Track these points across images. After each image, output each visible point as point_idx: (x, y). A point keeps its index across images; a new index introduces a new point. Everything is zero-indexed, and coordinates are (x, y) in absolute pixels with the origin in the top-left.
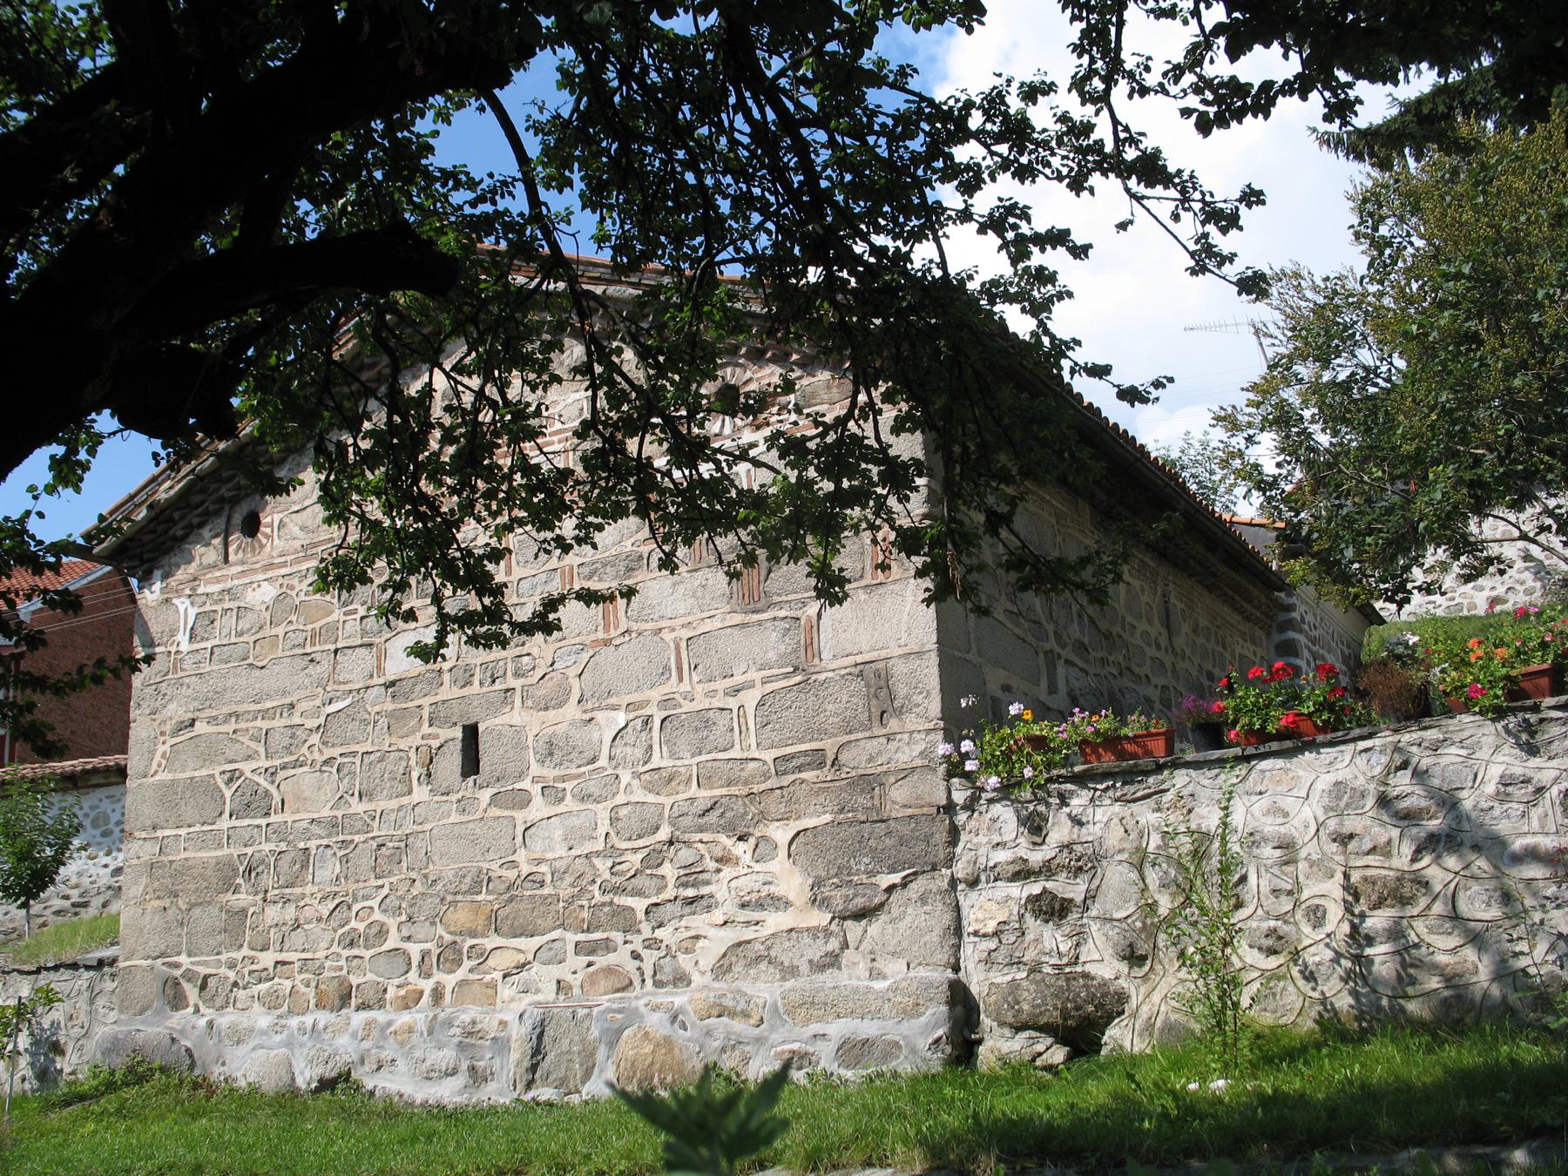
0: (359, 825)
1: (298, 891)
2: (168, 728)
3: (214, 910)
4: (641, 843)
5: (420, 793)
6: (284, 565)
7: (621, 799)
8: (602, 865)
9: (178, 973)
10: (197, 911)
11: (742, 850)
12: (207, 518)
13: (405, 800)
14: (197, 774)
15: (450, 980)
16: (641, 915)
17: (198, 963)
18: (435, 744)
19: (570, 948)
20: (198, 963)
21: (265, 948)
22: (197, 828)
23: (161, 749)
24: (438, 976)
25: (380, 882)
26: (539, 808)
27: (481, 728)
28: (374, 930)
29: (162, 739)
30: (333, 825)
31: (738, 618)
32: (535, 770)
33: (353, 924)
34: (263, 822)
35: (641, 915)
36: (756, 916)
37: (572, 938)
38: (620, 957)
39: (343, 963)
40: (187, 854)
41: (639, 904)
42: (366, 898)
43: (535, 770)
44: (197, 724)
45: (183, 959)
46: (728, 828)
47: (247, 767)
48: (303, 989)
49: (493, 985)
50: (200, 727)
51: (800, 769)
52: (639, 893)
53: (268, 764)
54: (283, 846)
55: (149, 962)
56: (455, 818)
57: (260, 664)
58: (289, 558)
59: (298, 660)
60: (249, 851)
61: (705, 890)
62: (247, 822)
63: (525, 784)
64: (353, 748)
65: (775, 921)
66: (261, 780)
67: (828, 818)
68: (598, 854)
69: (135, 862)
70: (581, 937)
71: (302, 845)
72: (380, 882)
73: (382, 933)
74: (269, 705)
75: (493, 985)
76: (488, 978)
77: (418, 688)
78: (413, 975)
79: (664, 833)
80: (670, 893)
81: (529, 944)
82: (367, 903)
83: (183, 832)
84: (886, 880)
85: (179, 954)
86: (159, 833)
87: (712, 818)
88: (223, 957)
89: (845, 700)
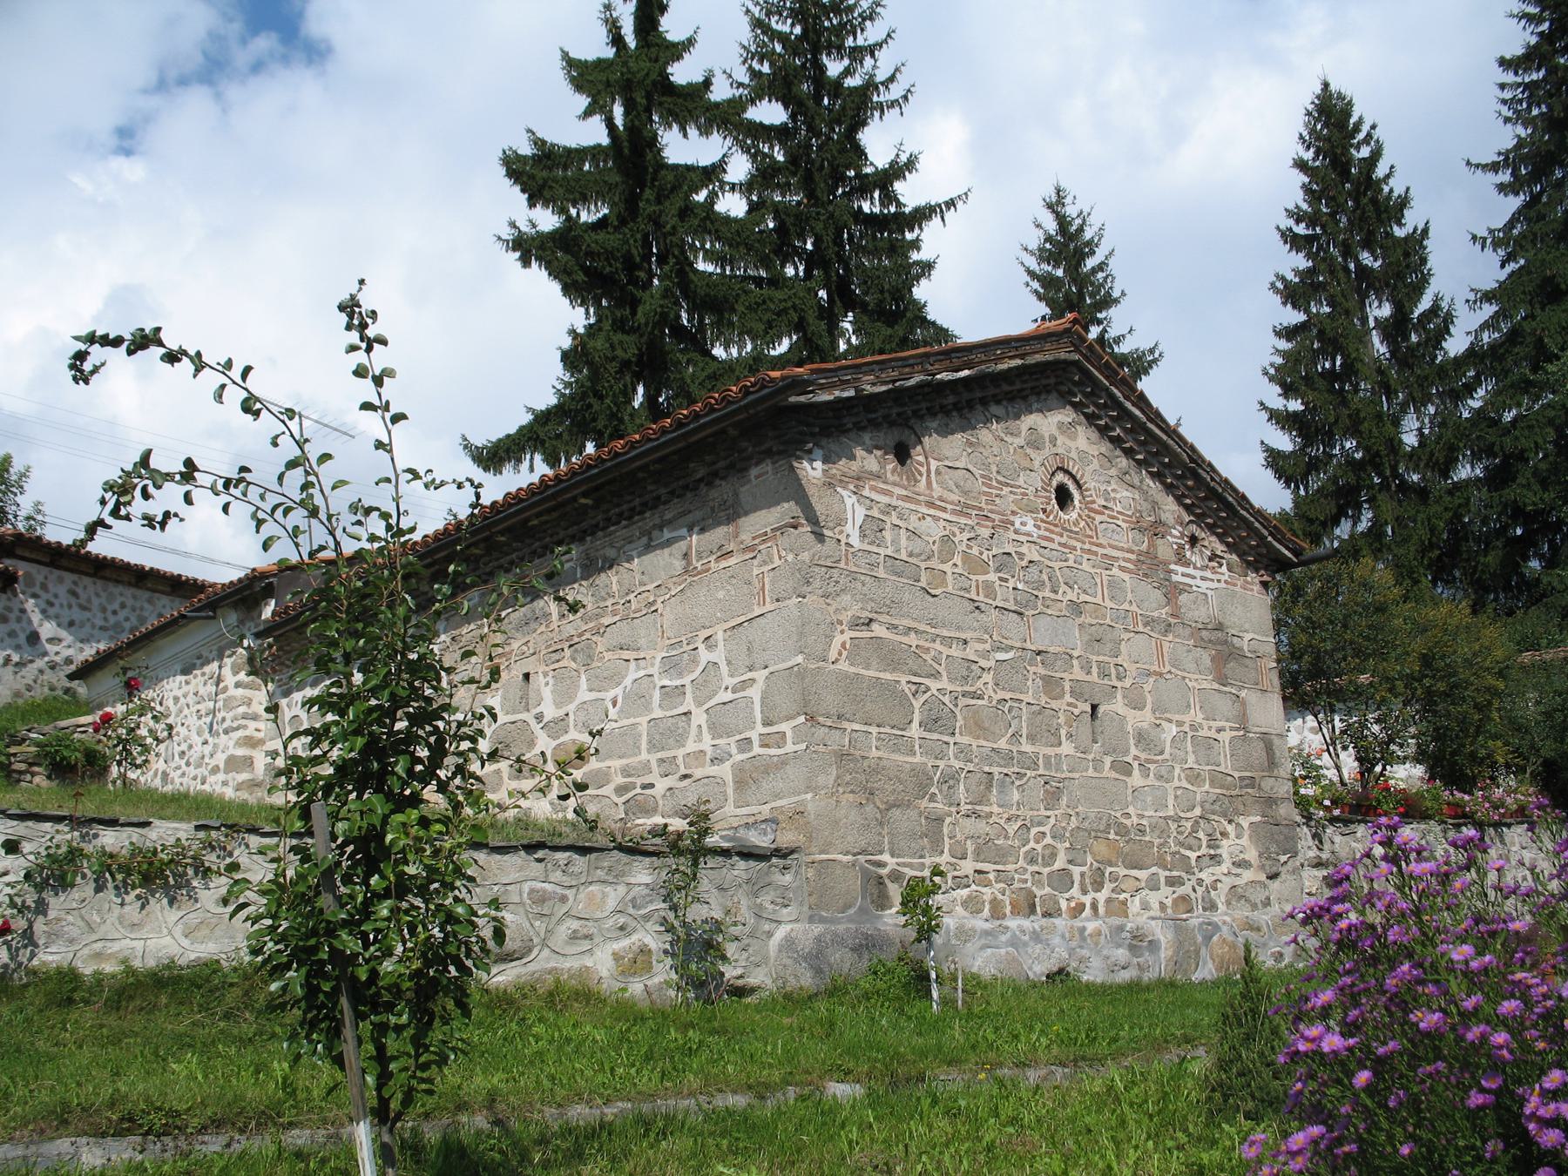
0: (1028, 762)
1: (987, 809)
2: (846, 617)
3: (913, 814)
4: (1189, 815)
5: (1067, 748)
6: (944, 510)
7: (1176, 783)
8: (1173, 826)
9: (884, 872)
10: (896, 812)
11: (1230, 828)
12: (874, 425)
13: (1058, 750)
14: (881, 675)
15: (1102, 896)
16: (1193, 863)
17: (904, 865)
18: (1076, 712)
19: (1162, 880)
20: (904, 865)
21: (964, 857)
22: (887, 730)
23: (838, 640)
24: (1092, 894)
25: (1048, 813)
26: (1136, 779)
27: (1101, 709)
28: (1047, 852)
29: (839, 628)
30: (1009, 758)
31: (1216, 686)
32: (1134, 751)
33: (1032, 844)
34: (951, 740)
35: (1193, 863)
36: (1239, 871)
37: (1163, 874)
38: (1185, 890)
39: (1028, 876)
40: (880, 754)
41: (1193, 855)
42: (1040, 824)
43: (1134, 751)
44: (874, 626)
45: (886, 857)
46: (1224, 815)
47: (934, 685)
48: (1000, 897)
49: (1124, 903)
50: (878, 630)
51: (1247, 786)
52: (1190, 848)
53: (950, 688)
54: (970, 767)
55: (850, 857)
56: (1091, 772)
57: (933, 592)
58: (949, 507)
59: (967, 603)
60: (942, 764)
61: (1219, 851)
62: (935, 736)
63: (1129, 759)
64: (1021, 697)
65: (1248, 875)
66: (946, 699)
67: (1259, 818)
68: (1169, 817)
69: (821, 748)
70: (1167, 873)
71: (987, 769)
72: (1048, 813)
73: (1054, 856)
74: (945, 633)
75: (1124, 903)
76: (1122, 897)
77: (1059, 663)
78: (1075, 891)
79: (1198, 811)
80: (1204, 850)
81: (1143, 874)
82: (1042, 829)
83: (874, 730)
84: (1283, 858)
85: (881, 852)
86: (849, 726)
87: (1216, 807)
88: (927, 861)
89: (1258, 752)
